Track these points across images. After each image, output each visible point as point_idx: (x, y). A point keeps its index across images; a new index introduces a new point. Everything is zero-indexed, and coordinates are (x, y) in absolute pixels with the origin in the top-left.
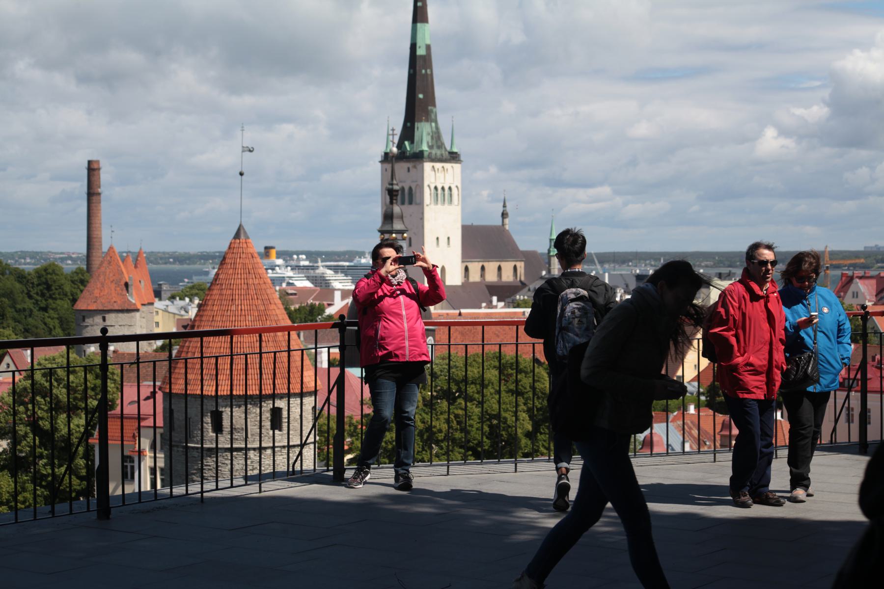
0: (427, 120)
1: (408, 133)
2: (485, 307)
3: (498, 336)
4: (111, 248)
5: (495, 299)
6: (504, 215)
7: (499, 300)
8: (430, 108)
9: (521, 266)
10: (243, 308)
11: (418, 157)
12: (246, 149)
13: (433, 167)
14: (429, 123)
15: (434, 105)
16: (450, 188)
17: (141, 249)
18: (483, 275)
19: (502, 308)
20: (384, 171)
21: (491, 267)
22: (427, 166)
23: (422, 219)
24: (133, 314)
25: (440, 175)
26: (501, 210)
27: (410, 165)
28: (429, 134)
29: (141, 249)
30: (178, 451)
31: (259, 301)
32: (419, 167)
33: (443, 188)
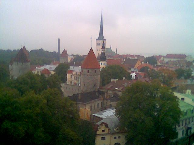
4: (64, 50)
6: (111, 47)
20: (96, 42)
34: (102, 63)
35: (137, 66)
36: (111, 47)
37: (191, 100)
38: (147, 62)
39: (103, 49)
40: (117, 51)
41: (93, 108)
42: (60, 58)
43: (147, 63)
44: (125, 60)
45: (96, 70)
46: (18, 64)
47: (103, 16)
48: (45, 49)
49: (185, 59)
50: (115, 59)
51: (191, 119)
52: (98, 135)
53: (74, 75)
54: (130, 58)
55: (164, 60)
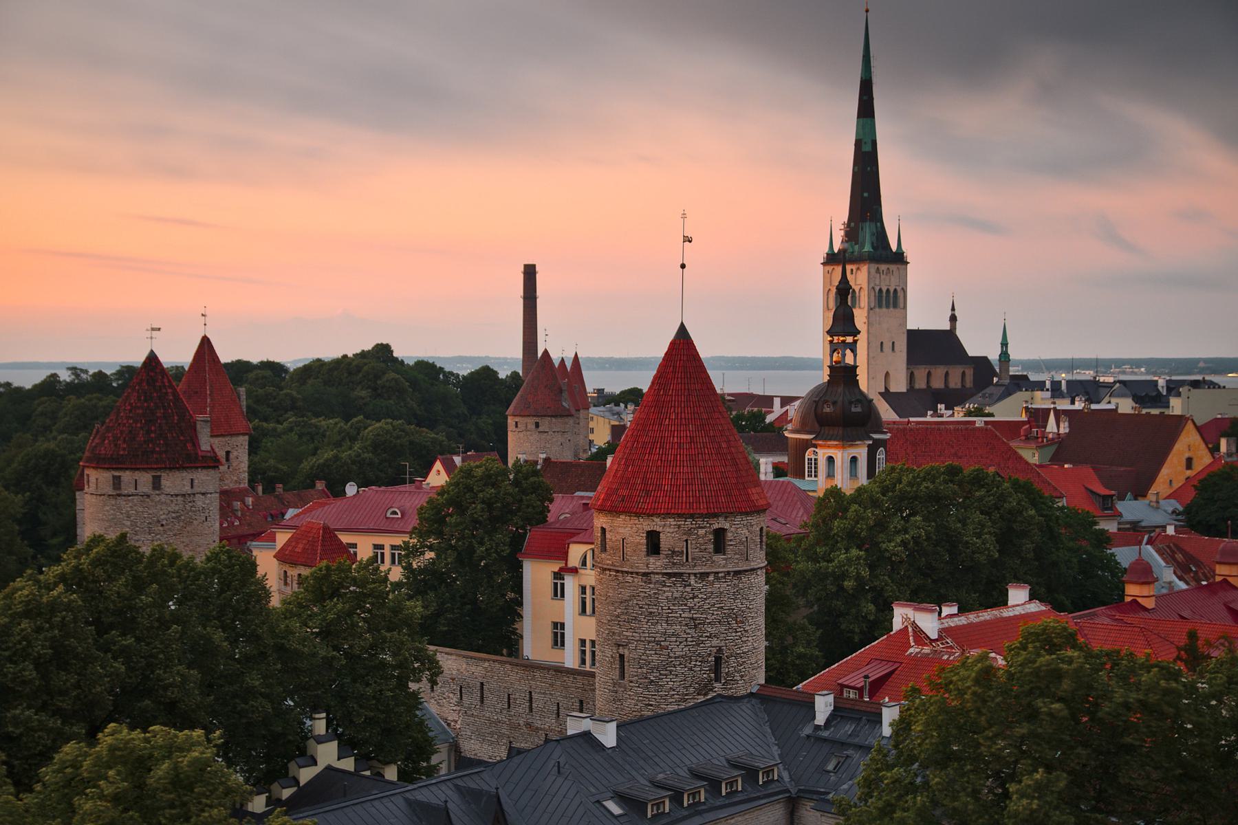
0: (871, 220)
1: (851, 233)
2: (932, 416)
3: (953, 447)
4: (546, 352)
5: (941, 407)
6: (953, 319)
8: (875, 207)
9: (970, 373)
10: (683, 416)
12: (687, 239)
13: (878, 268)
14: (873, 225)
16: (895, 290)
17: (576, 354)
18: (928, 382)
21: (939, 372)
24: (566, 420)
26: (949, 313)
27: (854, 267)
28: (873, 234)
29: (576, 354)
30: (610, 575)
31: (702, 408)
33: (888, 290)
34: (831, 460)
35: (1172, 473)
36: (953, 319)
40: (1009, 341)
42: (511, 421)
44: (1064, 428)
46: (117, 482)
48: (407, 351)
50: (979, 422)
53: (574, 571)
54: (1126, 406)
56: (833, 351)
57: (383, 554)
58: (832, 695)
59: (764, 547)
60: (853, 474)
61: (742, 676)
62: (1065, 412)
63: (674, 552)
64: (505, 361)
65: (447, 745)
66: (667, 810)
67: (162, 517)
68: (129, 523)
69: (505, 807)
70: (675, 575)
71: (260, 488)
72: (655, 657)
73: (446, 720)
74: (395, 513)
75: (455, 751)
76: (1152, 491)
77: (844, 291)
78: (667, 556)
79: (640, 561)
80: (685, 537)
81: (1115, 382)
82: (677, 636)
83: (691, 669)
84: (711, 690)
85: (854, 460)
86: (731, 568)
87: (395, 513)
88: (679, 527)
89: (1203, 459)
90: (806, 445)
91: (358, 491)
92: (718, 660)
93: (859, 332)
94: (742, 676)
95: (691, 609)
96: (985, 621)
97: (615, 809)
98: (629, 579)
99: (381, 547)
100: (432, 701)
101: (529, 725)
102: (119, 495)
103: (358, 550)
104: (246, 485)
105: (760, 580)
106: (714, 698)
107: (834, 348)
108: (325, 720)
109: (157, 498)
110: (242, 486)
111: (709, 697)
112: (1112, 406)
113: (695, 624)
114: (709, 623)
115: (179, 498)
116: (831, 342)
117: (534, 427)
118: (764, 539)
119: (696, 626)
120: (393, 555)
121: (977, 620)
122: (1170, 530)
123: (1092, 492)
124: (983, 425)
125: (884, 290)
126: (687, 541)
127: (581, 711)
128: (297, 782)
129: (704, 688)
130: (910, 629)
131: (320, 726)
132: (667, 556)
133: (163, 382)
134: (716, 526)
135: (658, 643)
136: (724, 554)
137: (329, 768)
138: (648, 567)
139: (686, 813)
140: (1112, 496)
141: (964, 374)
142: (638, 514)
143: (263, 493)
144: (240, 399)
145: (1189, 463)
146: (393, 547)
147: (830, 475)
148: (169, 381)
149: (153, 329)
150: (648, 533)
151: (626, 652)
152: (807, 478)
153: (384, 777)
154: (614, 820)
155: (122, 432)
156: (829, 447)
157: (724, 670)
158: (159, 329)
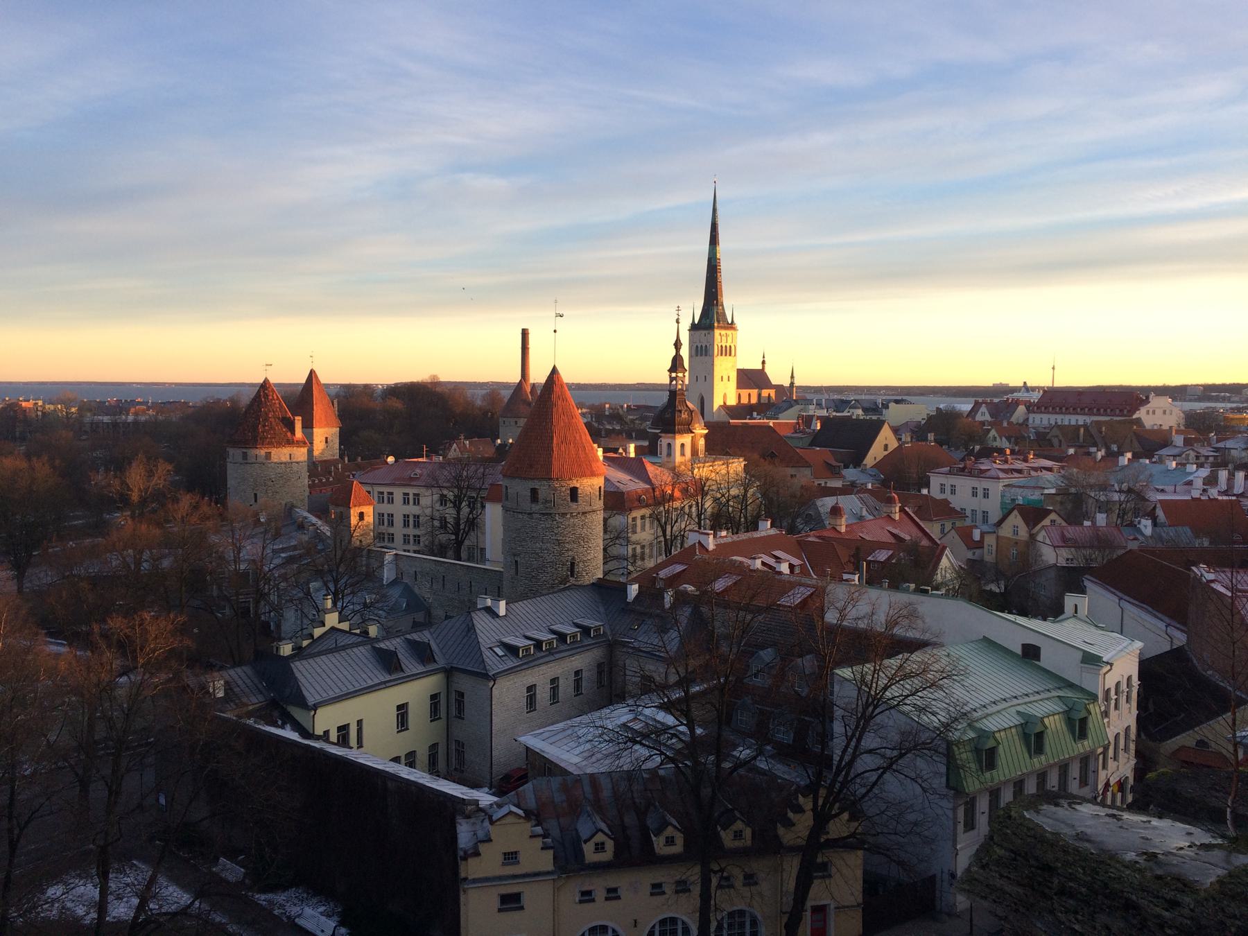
2: (749, 419)
5: (755, 414)
6: (764, 362)
7: (757, 415)
11: (710, 328)
15: (722, 296)
16: (730, 346)
19: (760, 419)
20: (691, 337)
21: (754, 392)
22: (717, 332)
23: (713, 365)
25: (724, 338)
27: (706, 332)
32: (711, 333)
33: (726, 346)
34: (669, 445)
35: (876, 452)
36: (764, 362)
37: (1079, 655)
38: (931, 436)
39: (674, 375)
40: (795, 375)
41: (543, 694)
42: (501, 420)
43: (926, 439)
45: (575, 483)
46: (245, 456)
47: (719, 213)
49: (1134, 417)
51: (1075, 771)
52: (475, 881)
55: (1031, 421)
56: (671, 381)
57: (408, 498)
58: (637, 585)
59: (602, 498)
60: (683, 454)
61: (587, 573)
62: (819, 418)
63: (546, 501)
64: (505, 386)
65: (423, 612)
66: (532, 652)
67: (273, 476)
68: (252, 480)
69: (399, 657)
70: (547, 514)
71: (346, 459)
72: (535, 562)
73: (423, 598)
74: (417, 475)
75: (429, 616)
76: (864, 462)
77: (678, 345)
78: (542, 503)
79: (527, 505)
80: (554, 492)
81: (852, 400)
82: (548, 550)
83: (556, 569)
84: (568, 581)
85: (683, 445)
86: (580, 509)
87: (416, 475)
88: (550, 485)
89: (894, 444)
90: (657, 437)
91: (396, 461)
92: (573, 564)
93: (686, 370)
94: (587, 573)
95: (556, 534)
96: (743, 540)
97: (500, 653)
98: (520, 516)
99: (408, 494)
100: (416, 586)
101: (470, 601)
102: (247, 463)
103: (394, 496)
104: (338, 457)
105: (600, 517)
106: (569, 586)
107: (672, 379)
108: (330, 600)
109: (269, 465)
110: (335, 457)
111: (567, 585)
112: (849, 414)
113: (559, 543)
114: (568, 543)
115: (283, 465)
116: (670, 377)
117: (514, 424)
118: (602, 493)
119: (559, 544)
120: (414, 499)
121: (738, 539)
122: (870, 486)
123: (827, 463)
124: (771, 425)
125: (699, 346)
126: (554, 494)
127: (486, 595)
128: (311, 636)
129: (564, 580)
130: (697, 545)
131: (329, 604)
132: (542, 503)
133: (273, 397)
134: (573, 486)
135: (537, 554)
136: (577, 502)
137: (333, 629)
138: (531, 509)
139: (543, 654)
140: (839, 467)
141: (749, 395)
142: (525, 479)
143: (349, 461)
144: (333, 405)
145: (886, 447)
146: (414, 494)
147: (669, 454)
148: (277, 397)
149: (267, 365)
150: (531, 489)
151: (519, 559)
152: (659, 455)
153: (368, 633)
154: (497, 658)
155: (248, 426)
156: (669, 438)
157: (576, 570)
158: (271, 365)
